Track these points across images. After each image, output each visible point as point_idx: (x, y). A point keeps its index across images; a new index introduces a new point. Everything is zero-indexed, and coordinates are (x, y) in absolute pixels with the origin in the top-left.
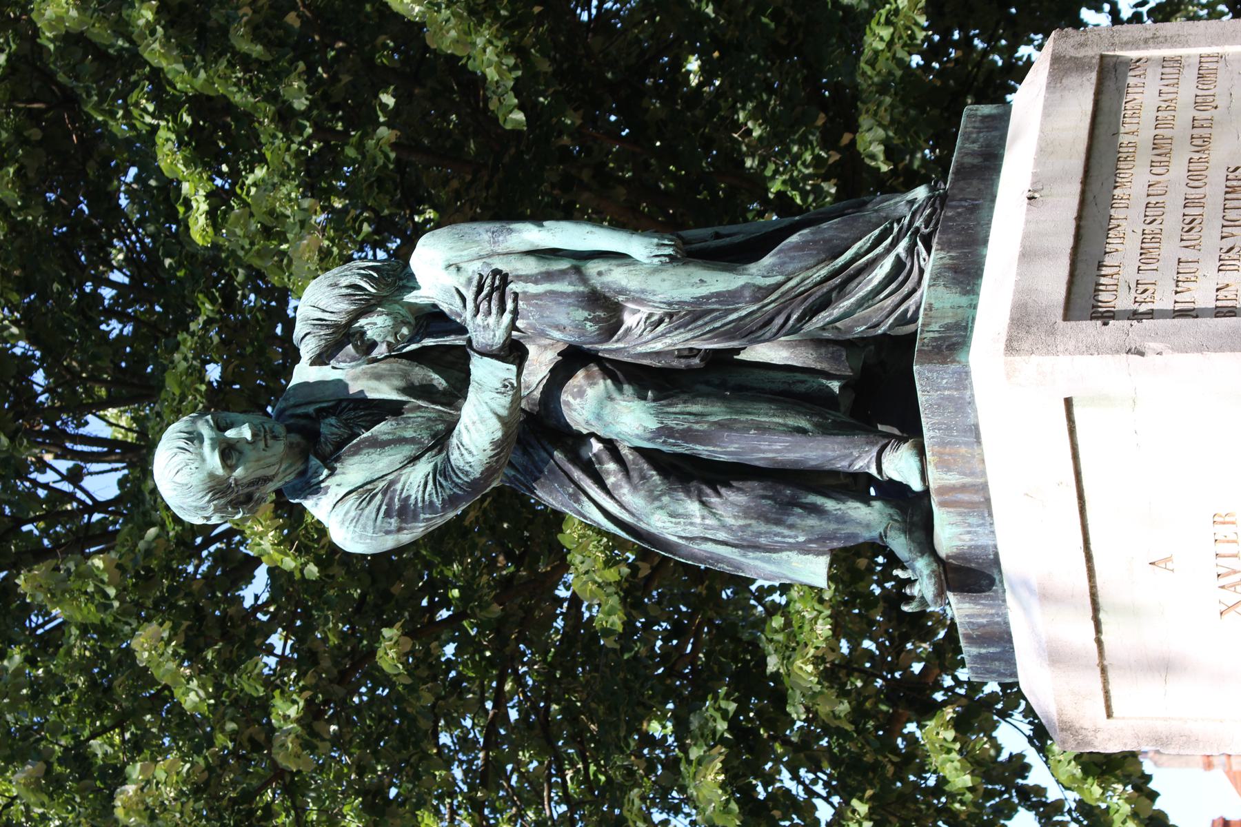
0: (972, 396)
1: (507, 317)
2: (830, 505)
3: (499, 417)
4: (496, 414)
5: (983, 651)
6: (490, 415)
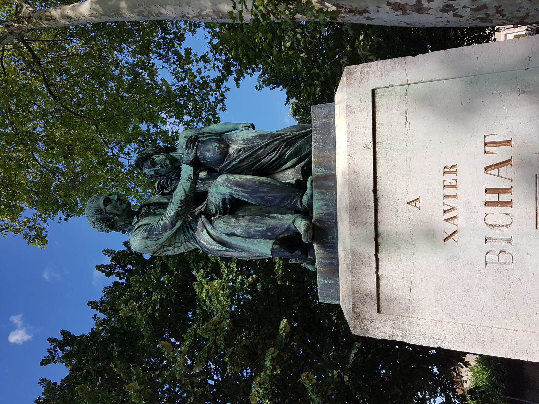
0: (334, 120)
1: (194, 150)
2: (279, 216)
3: (185, 191)
4: (184, 189)
5: (326, 282)
6: (182, 189)
